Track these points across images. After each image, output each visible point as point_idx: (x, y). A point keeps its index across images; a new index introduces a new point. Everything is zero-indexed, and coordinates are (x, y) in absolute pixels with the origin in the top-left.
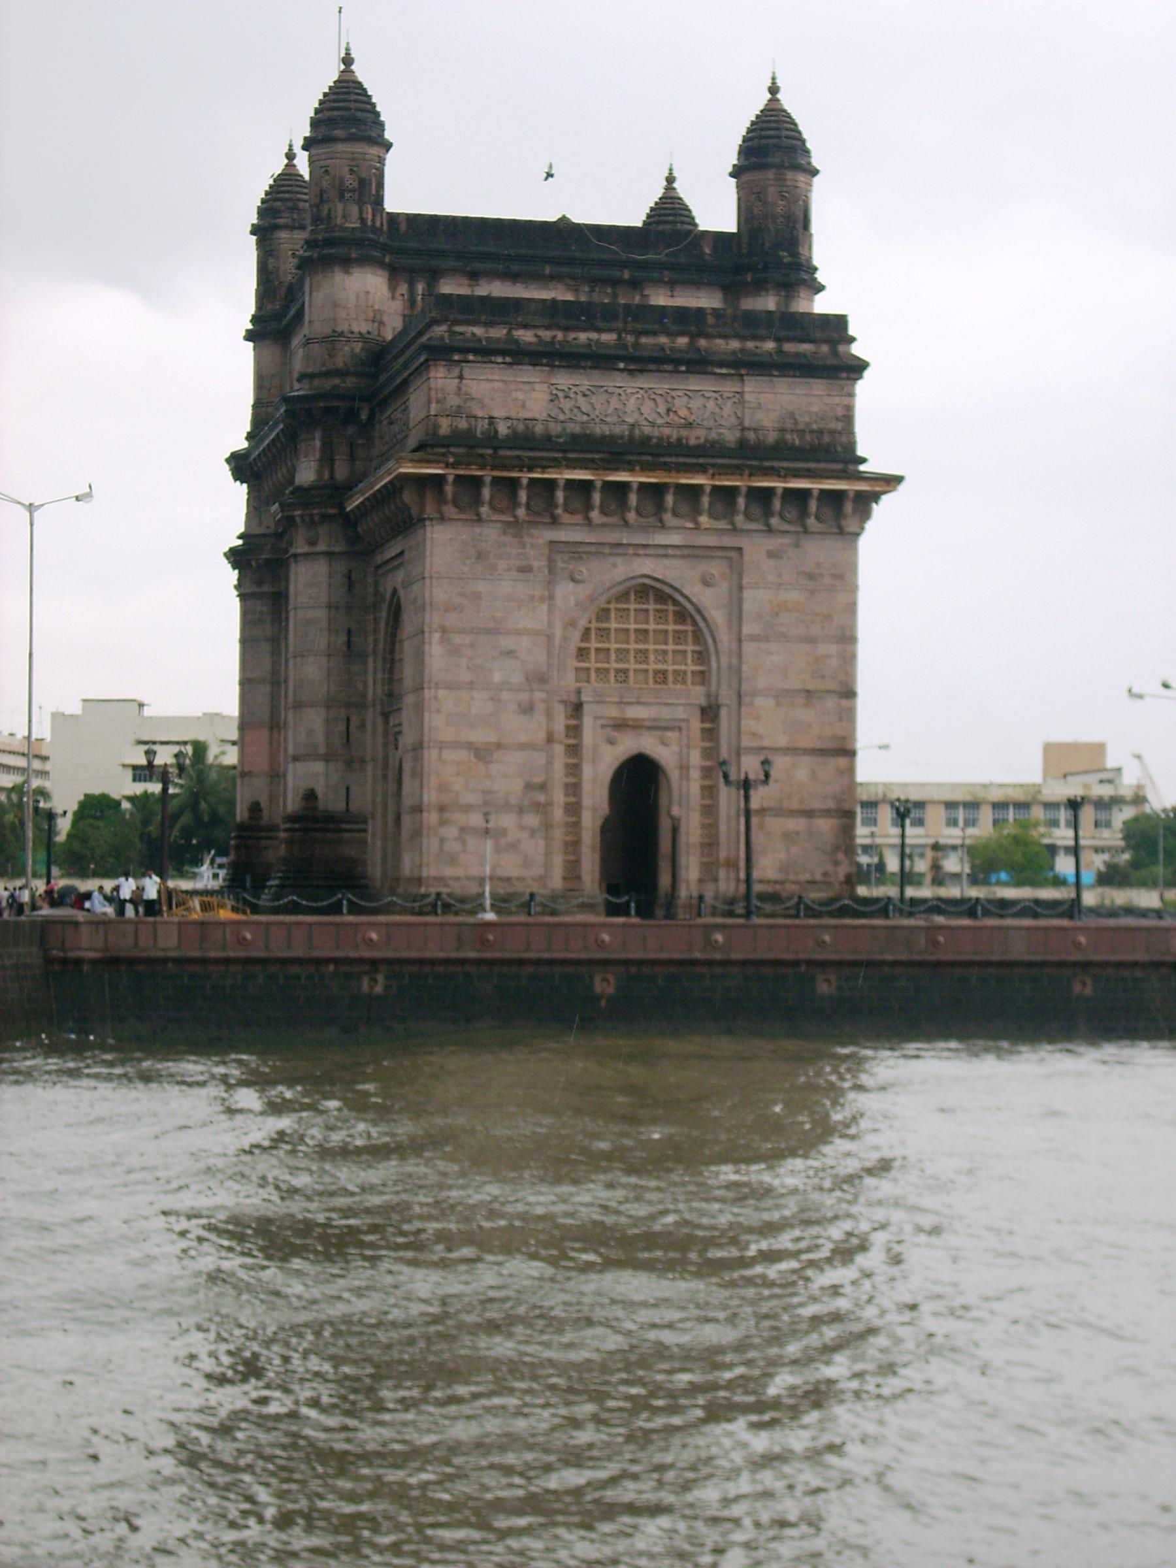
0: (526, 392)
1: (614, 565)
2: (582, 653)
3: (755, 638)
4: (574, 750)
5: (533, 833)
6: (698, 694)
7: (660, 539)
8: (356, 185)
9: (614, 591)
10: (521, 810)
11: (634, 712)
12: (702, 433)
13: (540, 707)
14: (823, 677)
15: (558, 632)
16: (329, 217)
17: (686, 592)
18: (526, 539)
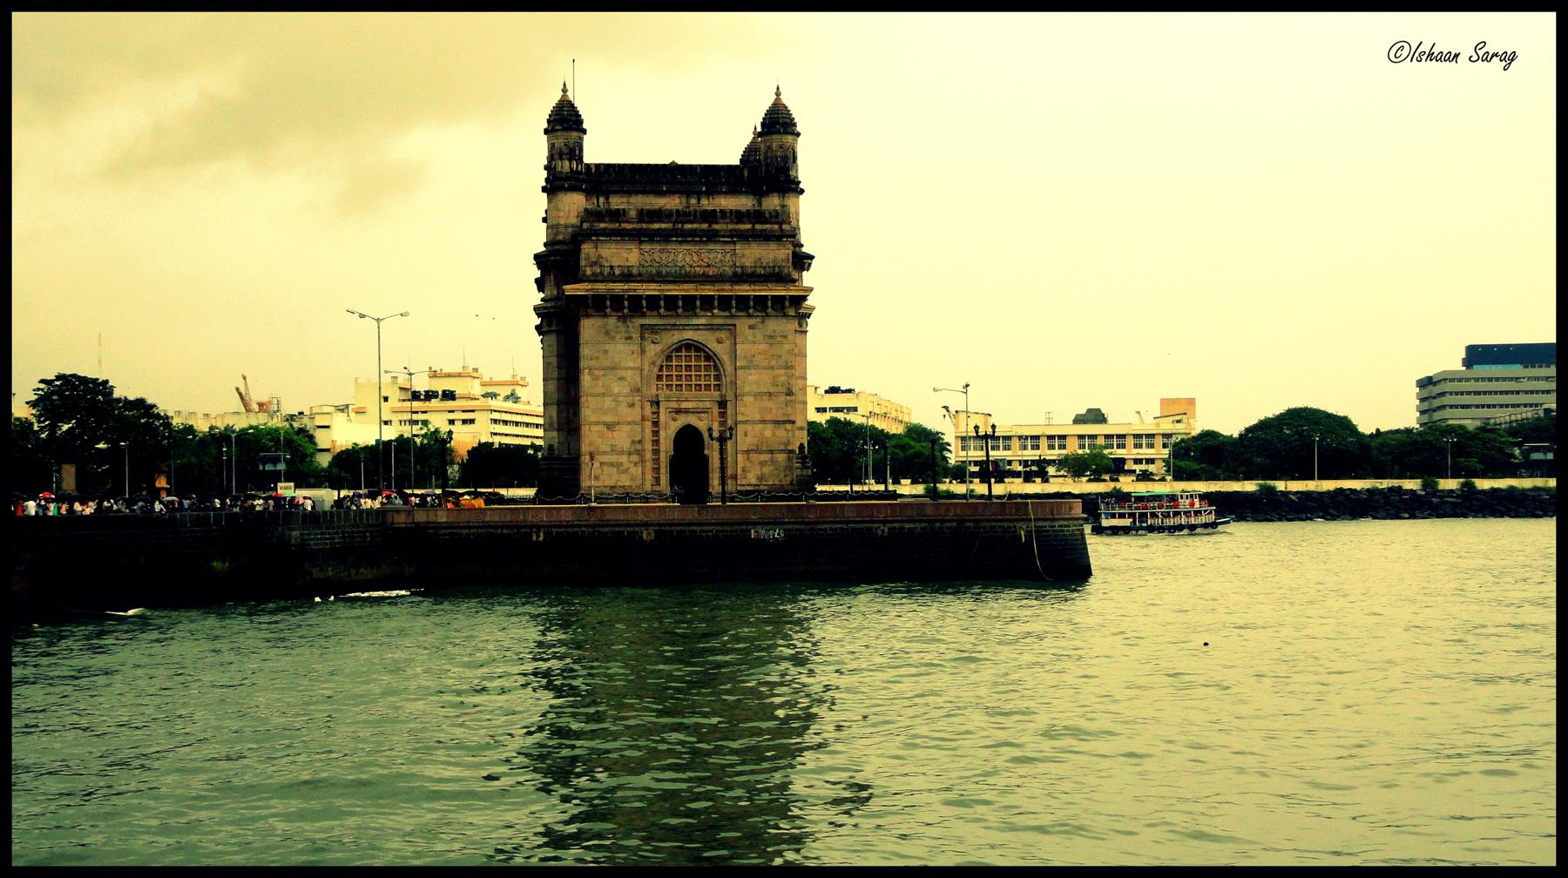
0: (628, 253)
1: (673, 335)
2: (659, 378)
3: (742, 368)
4: (656, 424)
5: (636, 464)
6: (716, 394)
7: (695, 321)
8: (567, 151)
9: (674, 347)
10: (630, 454)
11: (684, 405)
12: (716, 270)
13: (638, 405)
14: (777, 385)
15: (646, 368)
16: (555, 167)
17: (710, 347)
18: (629, 323)
